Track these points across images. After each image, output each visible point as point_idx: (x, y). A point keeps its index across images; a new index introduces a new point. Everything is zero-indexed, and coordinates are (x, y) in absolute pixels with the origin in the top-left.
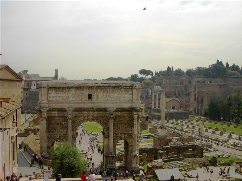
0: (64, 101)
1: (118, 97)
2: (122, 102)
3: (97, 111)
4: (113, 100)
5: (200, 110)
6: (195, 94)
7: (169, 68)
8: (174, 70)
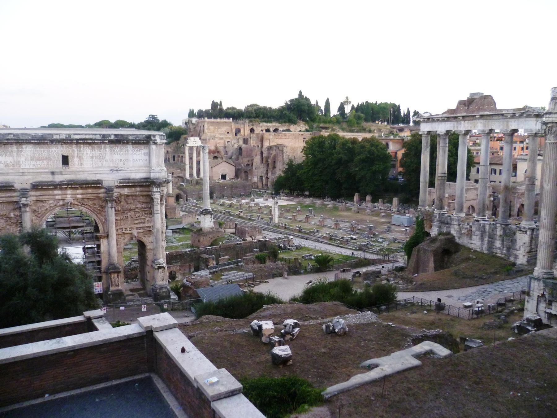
0: (12, 171)
1: (121, 160)
2: (130, 169)
3: (82, 188)
4: (112, 165)
5: (270, 180)
6: (262, 152)
7: (214, 105)
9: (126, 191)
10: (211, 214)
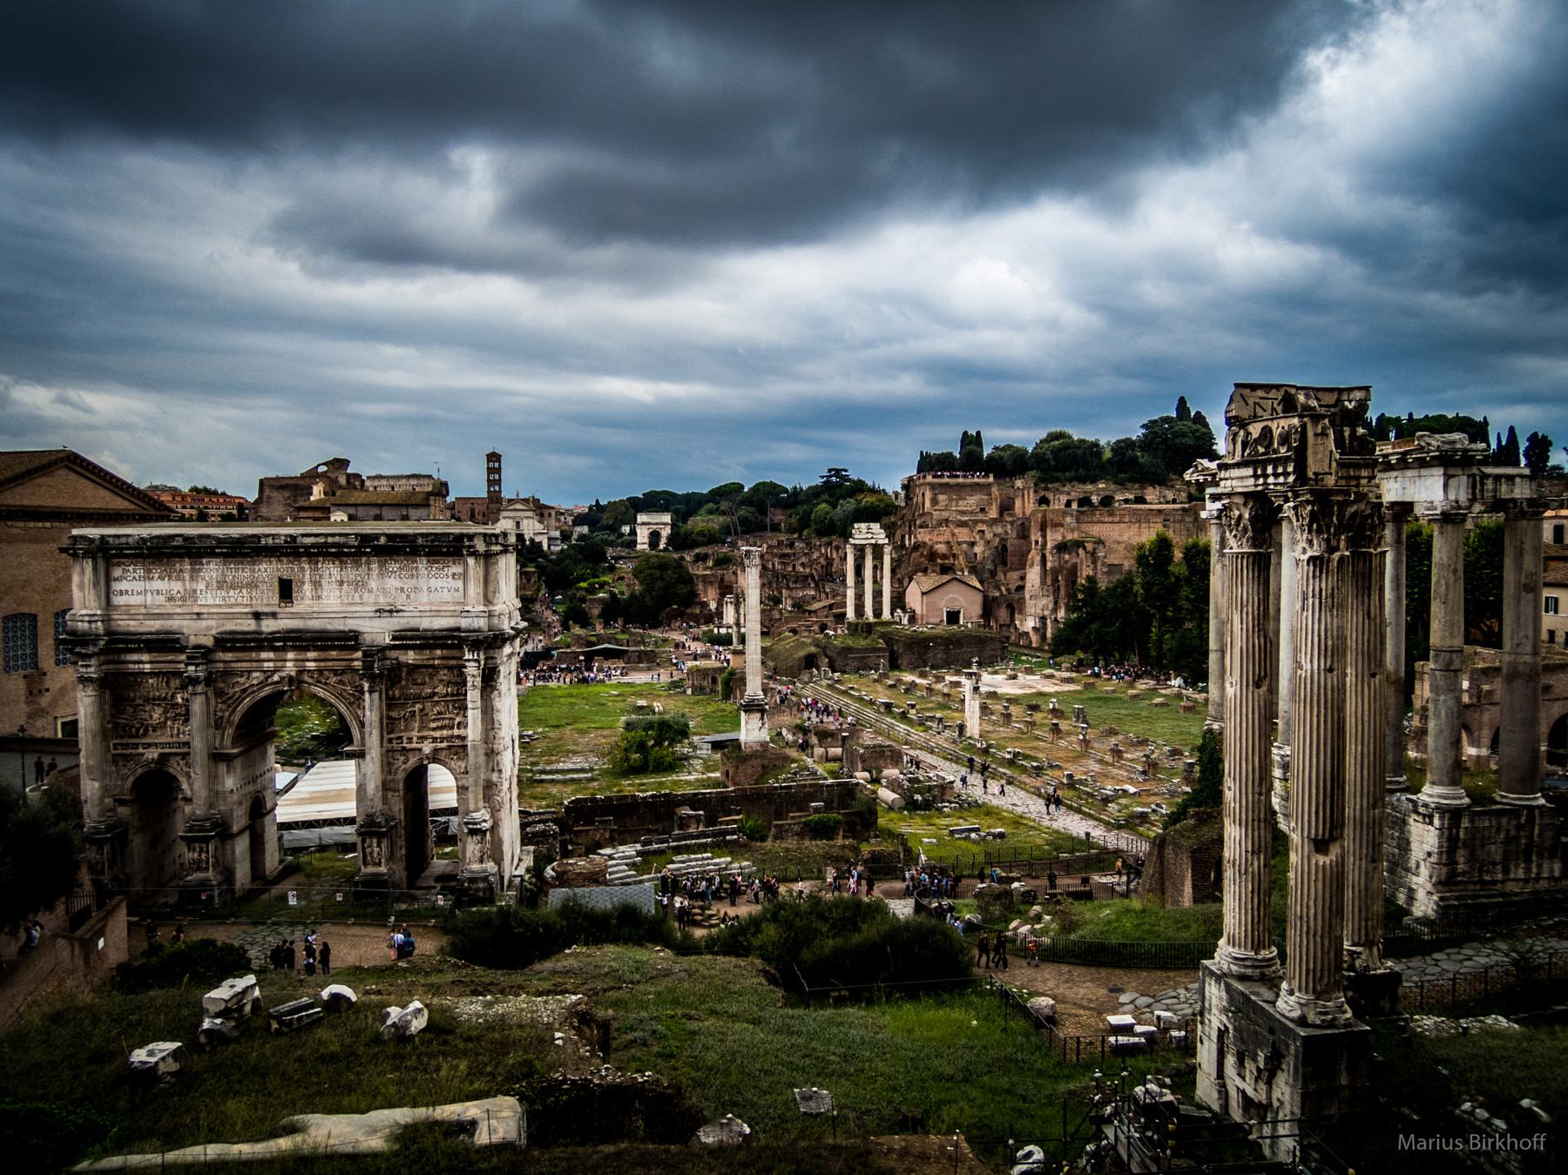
0: (178, 610)
1: (402, 590)
3: (317, 649)
4: (381, 600)
8: (987, 451)
9: (410, 657)
10: (763, 711)
